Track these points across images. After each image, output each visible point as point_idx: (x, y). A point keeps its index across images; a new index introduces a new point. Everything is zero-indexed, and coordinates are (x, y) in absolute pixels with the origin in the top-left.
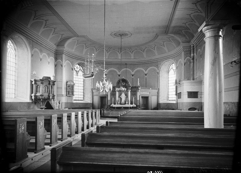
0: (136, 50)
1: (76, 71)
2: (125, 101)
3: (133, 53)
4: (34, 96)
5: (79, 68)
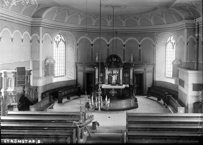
0: (128, 18)
1: (56, 42)
2: (116, 81)
3: (125, 20)
4: (4, 92)
5: (60, 38)
